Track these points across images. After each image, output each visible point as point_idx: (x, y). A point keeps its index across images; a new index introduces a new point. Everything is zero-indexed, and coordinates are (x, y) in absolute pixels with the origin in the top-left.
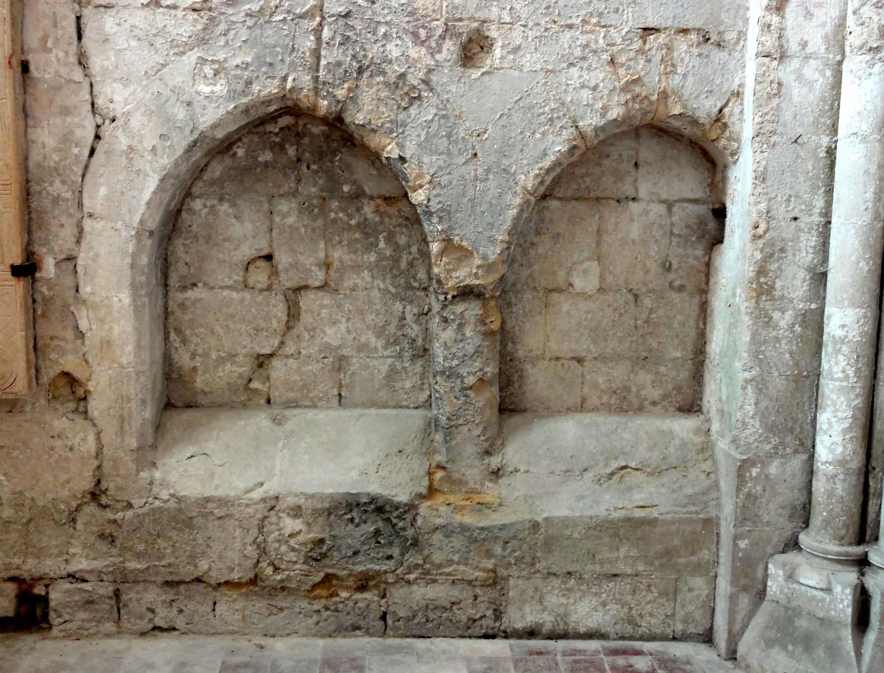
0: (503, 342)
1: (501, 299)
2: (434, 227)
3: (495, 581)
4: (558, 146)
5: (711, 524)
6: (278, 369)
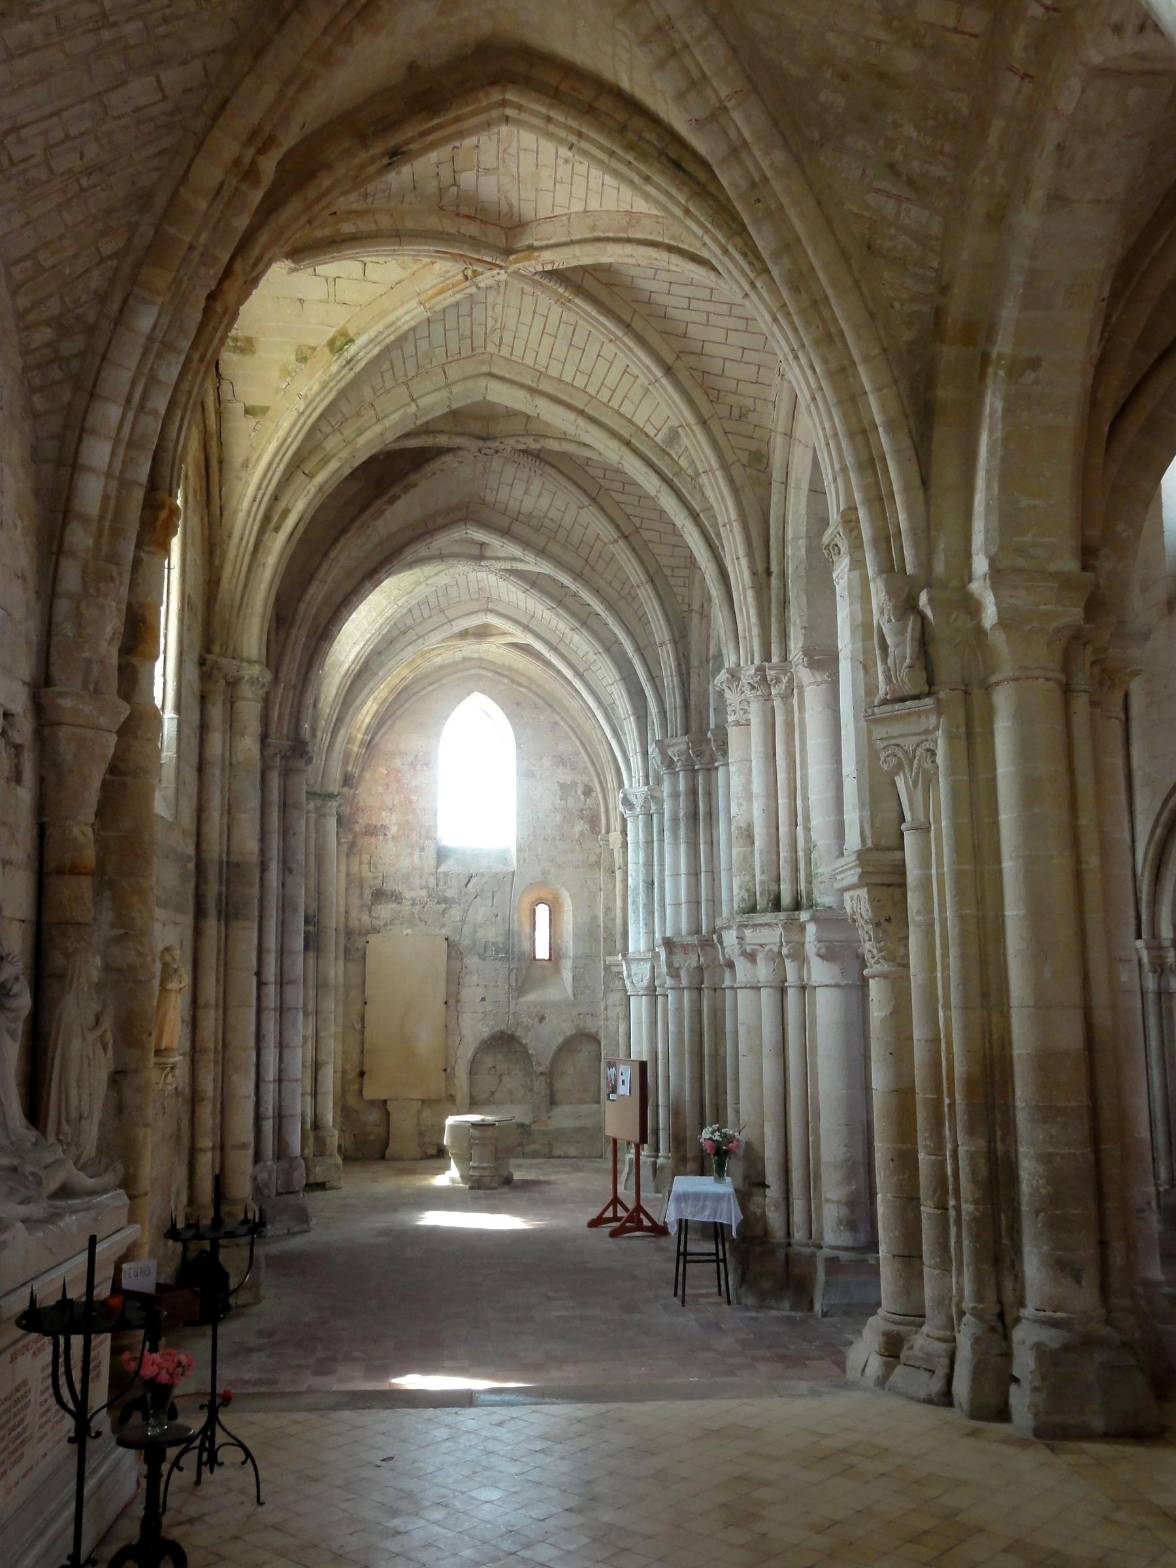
0: (551, 1086)
1: (550, 1075)
2: (534, 1059)
3: (550, 1144)
4: (561, 1040)
6: (497, 1095)
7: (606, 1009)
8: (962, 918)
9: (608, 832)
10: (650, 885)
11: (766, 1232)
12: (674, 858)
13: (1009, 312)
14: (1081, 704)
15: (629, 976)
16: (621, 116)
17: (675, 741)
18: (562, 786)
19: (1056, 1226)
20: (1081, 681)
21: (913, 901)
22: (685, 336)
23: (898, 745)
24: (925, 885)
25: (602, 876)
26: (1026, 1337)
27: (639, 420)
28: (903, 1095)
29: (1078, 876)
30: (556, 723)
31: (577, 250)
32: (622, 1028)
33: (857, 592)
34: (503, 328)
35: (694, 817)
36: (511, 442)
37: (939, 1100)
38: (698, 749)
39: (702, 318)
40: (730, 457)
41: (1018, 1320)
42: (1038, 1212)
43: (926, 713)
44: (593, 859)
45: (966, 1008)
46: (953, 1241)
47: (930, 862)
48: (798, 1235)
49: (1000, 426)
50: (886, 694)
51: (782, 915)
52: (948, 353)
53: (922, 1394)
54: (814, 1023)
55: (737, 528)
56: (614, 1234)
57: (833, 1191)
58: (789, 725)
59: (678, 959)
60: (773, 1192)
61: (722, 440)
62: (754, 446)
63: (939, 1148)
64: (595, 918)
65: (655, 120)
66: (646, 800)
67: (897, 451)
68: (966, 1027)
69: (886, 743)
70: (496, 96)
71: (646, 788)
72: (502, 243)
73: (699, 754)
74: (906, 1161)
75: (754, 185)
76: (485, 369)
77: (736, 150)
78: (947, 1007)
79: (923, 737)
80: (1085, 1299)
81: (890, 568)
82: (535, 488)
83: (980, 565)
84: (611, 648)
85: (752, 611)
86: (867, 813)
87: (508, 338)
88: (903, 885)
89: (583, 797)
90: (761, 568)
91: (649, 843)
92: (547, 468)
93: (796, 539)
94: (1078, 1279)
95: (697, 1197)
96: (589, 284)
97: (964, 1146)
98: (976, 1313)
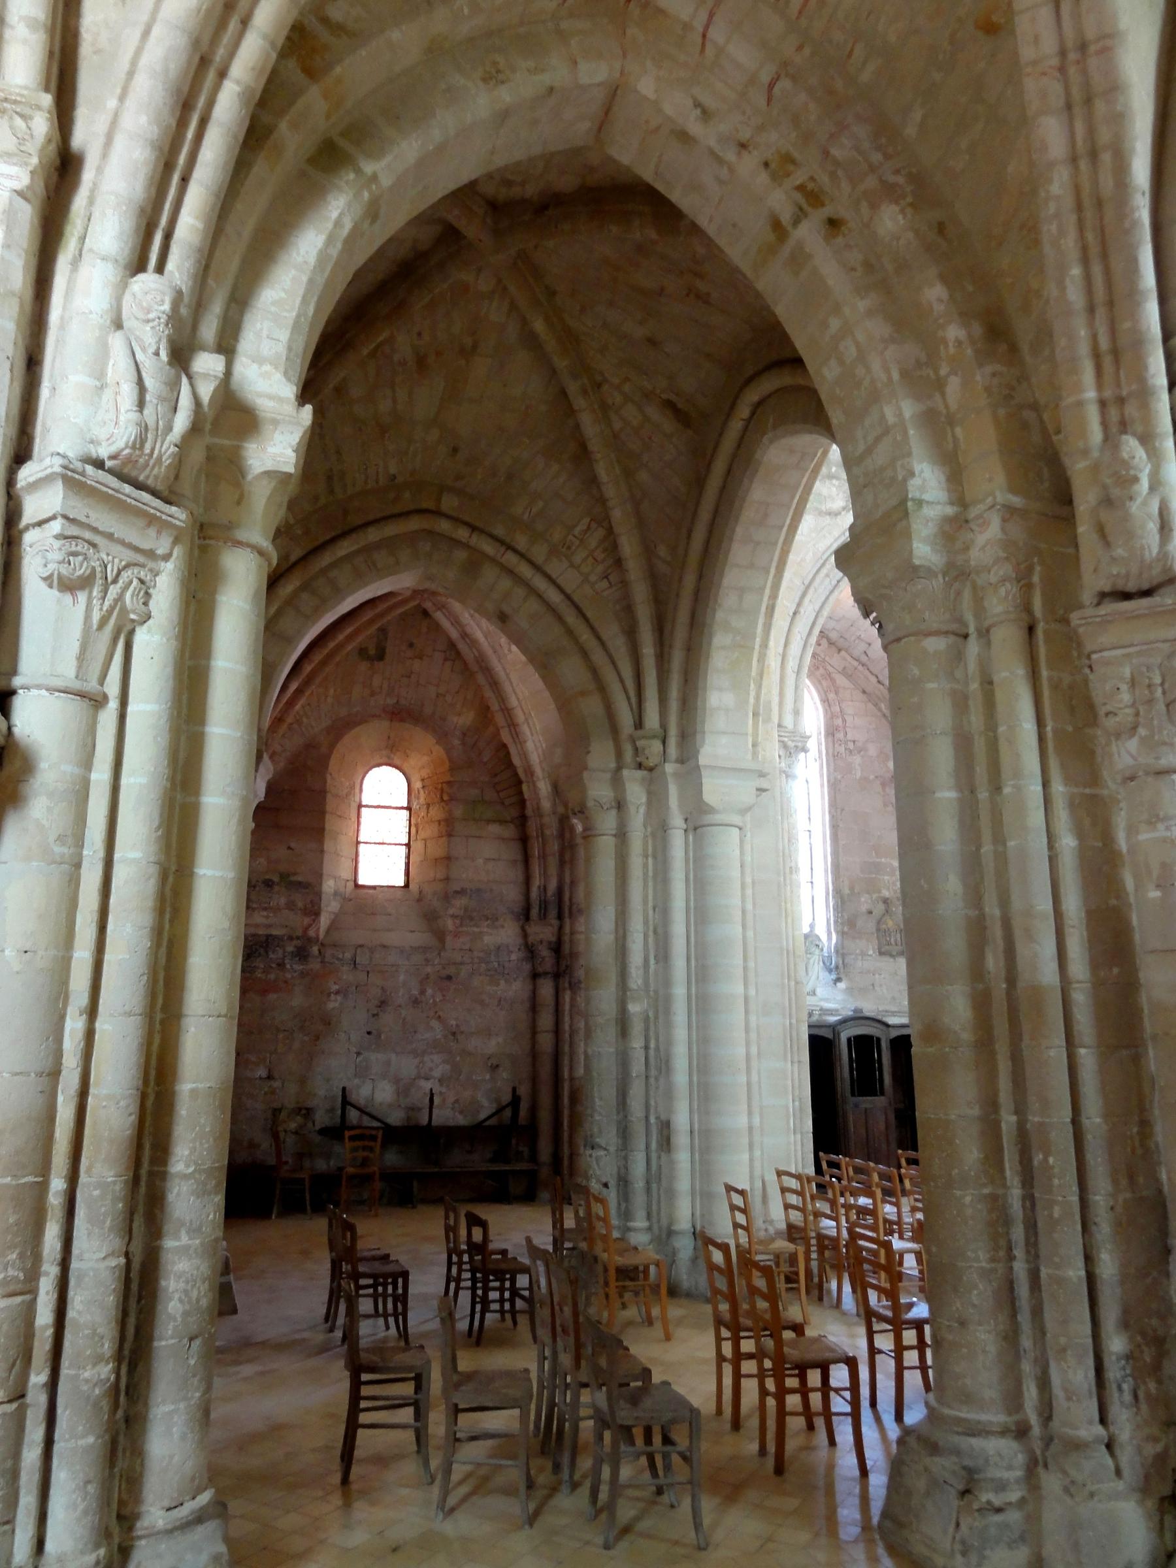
23: (94, 546)
37: (42, 1187)
42: (191, 1339)
49: (339, 245)
50: (112, 457)
79: (141, 559)
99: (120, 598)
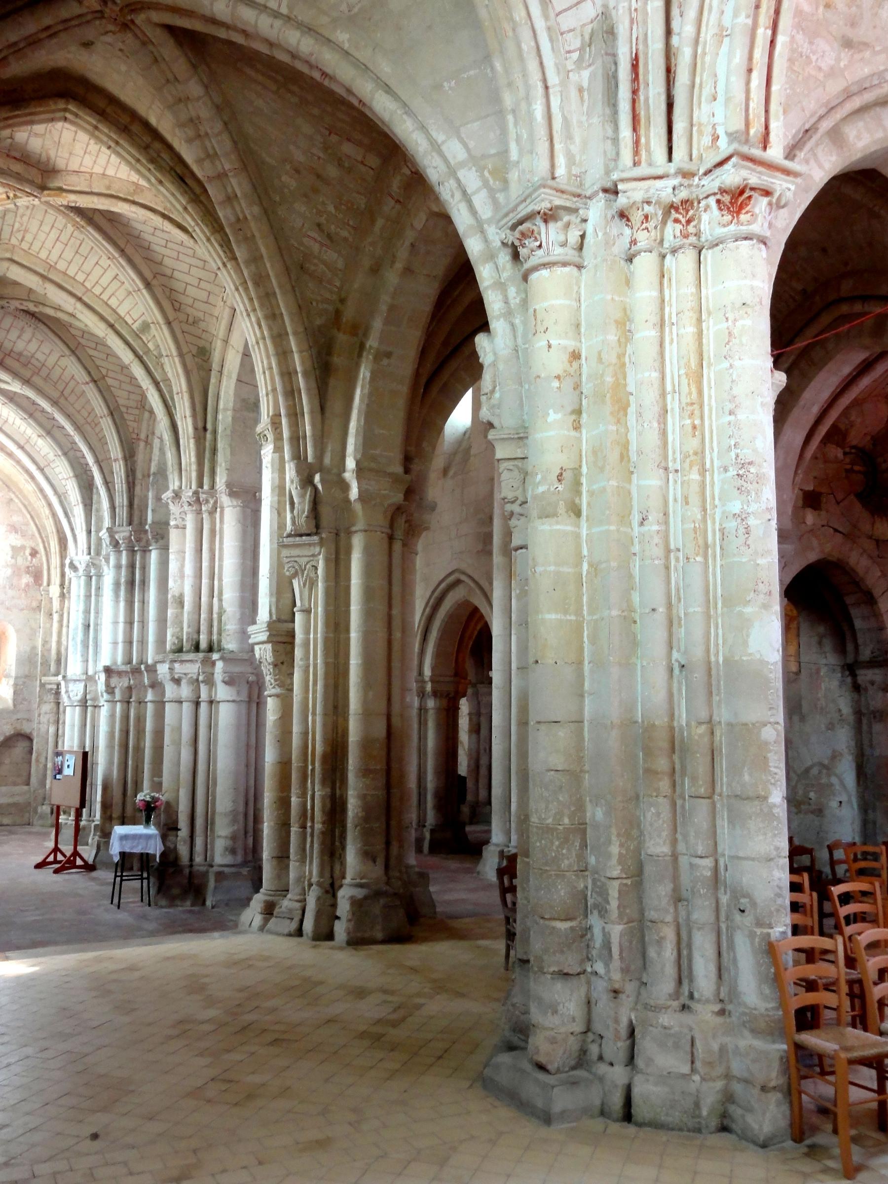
5: (30, 803)
7: (39, 715)
8: (326, 664)
9: (48, 585)
10: (87, 627)
11: (177, 858)
12: (110, 610)
13: (377, 324)
14: (397, 546)
15: (67, 692)
16: (147, 139)
17: (121, 529)
18: (13, 548)
19: (366, 834)
20: (399, 534)
21: (298, 653)
22: (161, 264)
24: (306, 643)
25: (42, 617)
26: (345, 895)
27: (122, 311)
28: (284, 765)
29: (390, 642)
30: (12, 499)
31: (95, 199)
32: (52, 730)
33: (277, 466)
34: (26, 231)
35: (131, 583)
36: (15, 304)
37: (306, 766)
38: (141, 535)
39: (175, 255)
40: (185, 350)
41: (341, 886)
42: (356, 827)
43: (314, 545)
44: (34, 604)
45: (325, 714)
46: (308, 846)
47: (310, 632)
48: (198, 859)
51: (201, 655)
52: (342, 338)
53: (286, 931)
54: (216, 725)
55: (186, 397)
56: (56, 871)
57: (223, 830)
58: (213, 532)
59: (114, 681)
60: (184, 833)
61: (180, 336)
62: (201, 343)
63: (304, 795)
64: (34, 648)
65: (169, 147)
66: (88, 566)
67: (308, 390)
68: (324, 725)
69: (289, 560)
70: (61, 104)
71: (89, 557)
72: (39, 180)
73: (139, 540)
74: (283, 803)
75: (238, 220)
76: (8, 255)
77: (230, 199)
78: (314, 714)
80: (377, 871)
81: (298, 457)
82: (27, 336)
83: (350, 464)
84: (70, 453)
85: (193, 454)
86: (274, 600)
87: (29, 237)
88: (292, 644)
89: (29, 558)
90: (200, 425)
91: (88, 597)
92: (41, 326)
93: (225, 409)
94: (374, 861)
95: (135, 837)
96: (97, 218)
97: (318, 792)
98: (319, 884)
99: (308, 575)
